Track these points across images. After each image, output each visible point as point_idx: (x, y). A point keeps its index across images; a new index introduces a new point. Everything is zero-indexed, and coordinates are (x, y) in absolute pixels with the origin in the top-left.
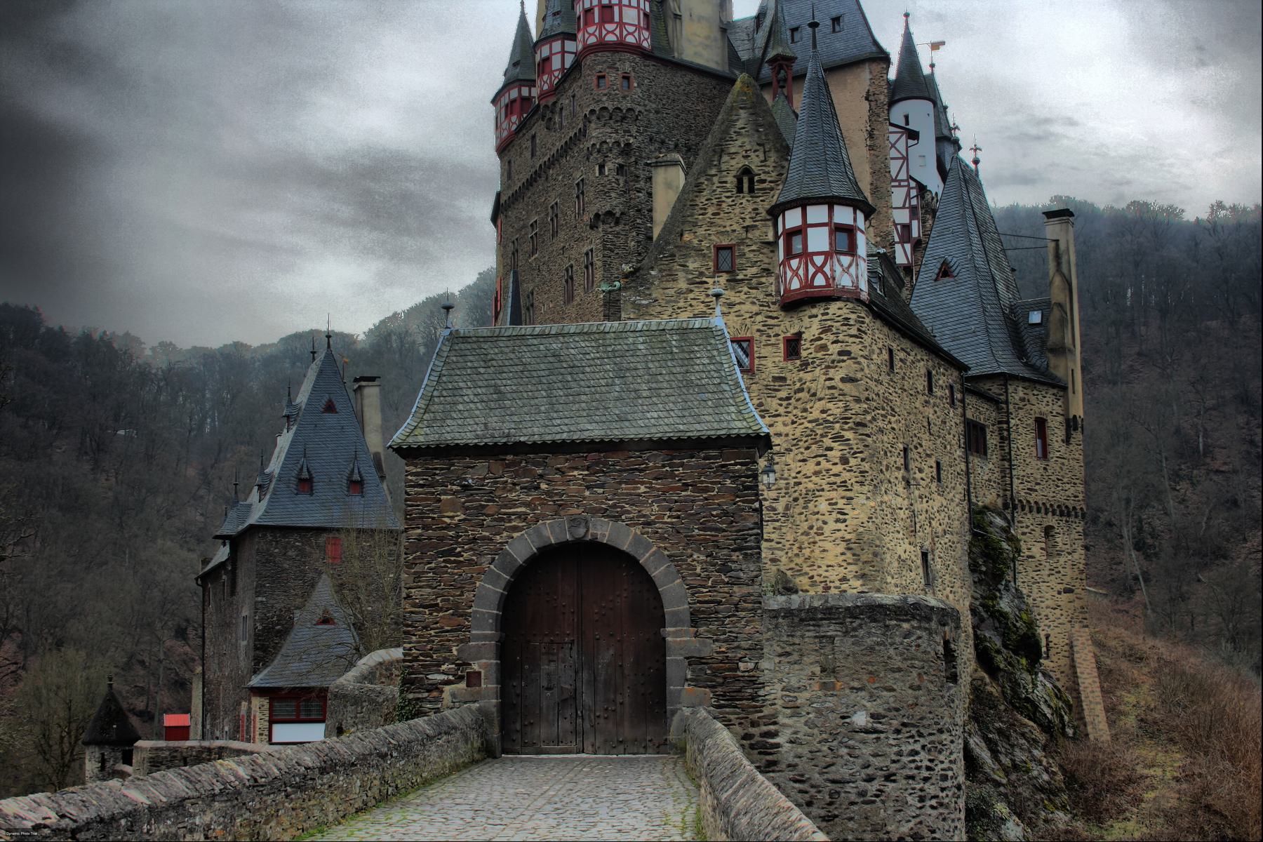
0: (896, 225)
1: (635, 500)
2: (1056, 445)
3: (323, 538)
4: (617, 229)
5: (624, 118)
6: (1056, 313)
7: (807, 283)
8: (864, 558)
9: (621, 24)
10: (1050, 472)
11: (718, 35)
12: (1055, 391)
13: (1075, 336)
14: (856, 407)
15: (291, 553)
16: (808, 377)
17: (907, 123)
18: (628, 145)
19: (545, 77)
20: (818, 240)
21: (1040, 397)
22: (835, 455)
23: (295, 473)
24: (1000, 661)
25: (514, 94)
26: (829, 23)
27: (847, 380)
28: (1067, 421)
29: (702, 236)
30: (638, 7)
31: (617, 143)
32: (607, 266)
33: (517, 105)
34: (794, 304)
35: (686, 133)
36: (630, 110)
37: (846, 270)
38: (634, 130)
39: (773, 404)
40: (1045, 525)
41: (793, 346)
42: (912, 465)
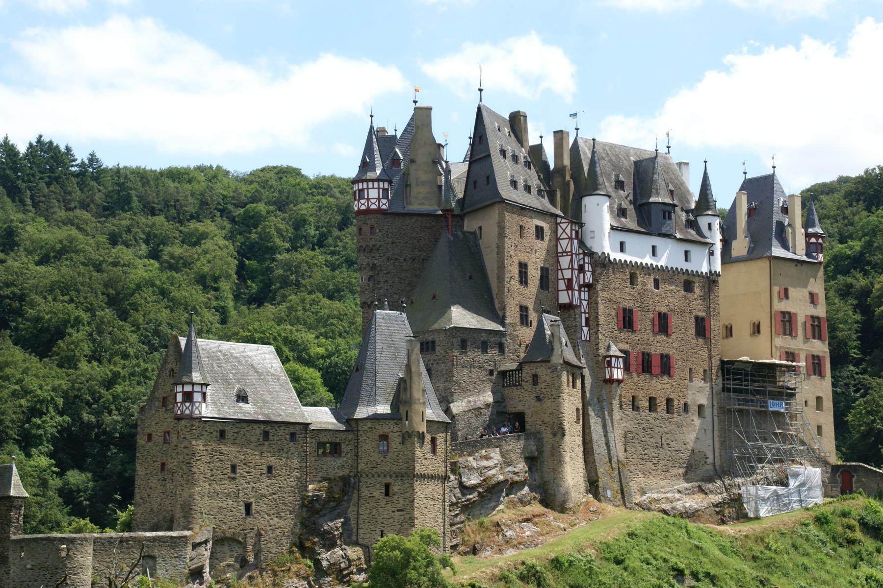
0: (564, 279)
2: (394, 446)
5: (371, 250)
8: (186, 510)
9: (368, 199)
10: (388, 458)
12: (395, 421)
14: (187, 457)
18: (374, 264)
20: (179, 398)
21: (384, 425)
22: (180, 474)
26: (485, 179)
27: (185, 448)
28: (403, 434)
30: (379, 188)
31: (368, 264)
34: (179, 418)
35: (412, 251)
36: (374, 245)
37: (187, 408)
38: (377, 256)
40: (385, 481)
42: (238, 471)
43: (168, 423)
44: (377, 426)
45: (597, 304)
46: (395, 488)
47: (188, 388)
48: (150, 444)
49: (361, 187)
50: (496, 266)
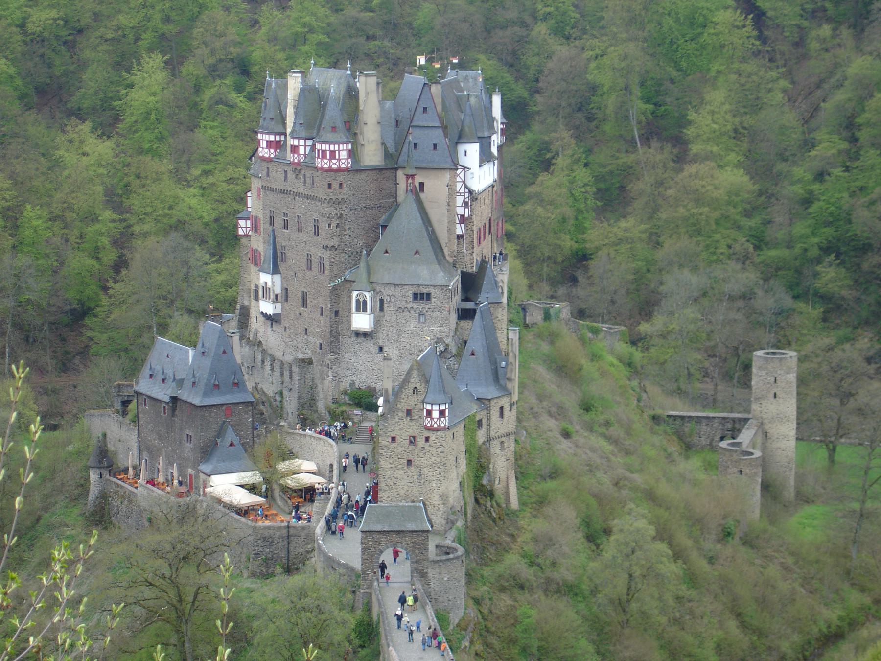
1: (406, 541)
3: (224, 408)
4: (336, 252)
5: (339, 203)
6: (509, 367)
7: (432, 426)
9: (339, 160)
11: (380, 146)
13: (516, 375)
14: (443, 459)
15: (213, 414)
16: (431, 449)
17: (466, 155)
18: (341, 214)
19: (296, 156)
20: (435, 414)
23: (213, 381)
24: (482, 501)
25: (272, 138)
29: (403, 406)
31: (337, 215)
32: (331, 270)
33: (273, 144)
34: (427, 428)
39: (421, 454)
41: (427, 439)
43: (412, 429)
44: (499, 401)
45: (473, 231)
46: (505, 444)
47: (442, 407)
48: (394, 445)
49: (332, 148)
50: (446, 220)
